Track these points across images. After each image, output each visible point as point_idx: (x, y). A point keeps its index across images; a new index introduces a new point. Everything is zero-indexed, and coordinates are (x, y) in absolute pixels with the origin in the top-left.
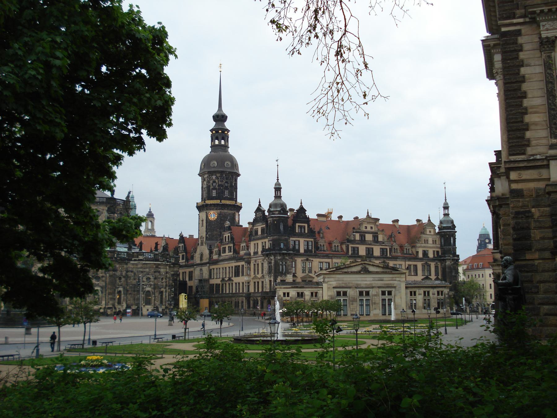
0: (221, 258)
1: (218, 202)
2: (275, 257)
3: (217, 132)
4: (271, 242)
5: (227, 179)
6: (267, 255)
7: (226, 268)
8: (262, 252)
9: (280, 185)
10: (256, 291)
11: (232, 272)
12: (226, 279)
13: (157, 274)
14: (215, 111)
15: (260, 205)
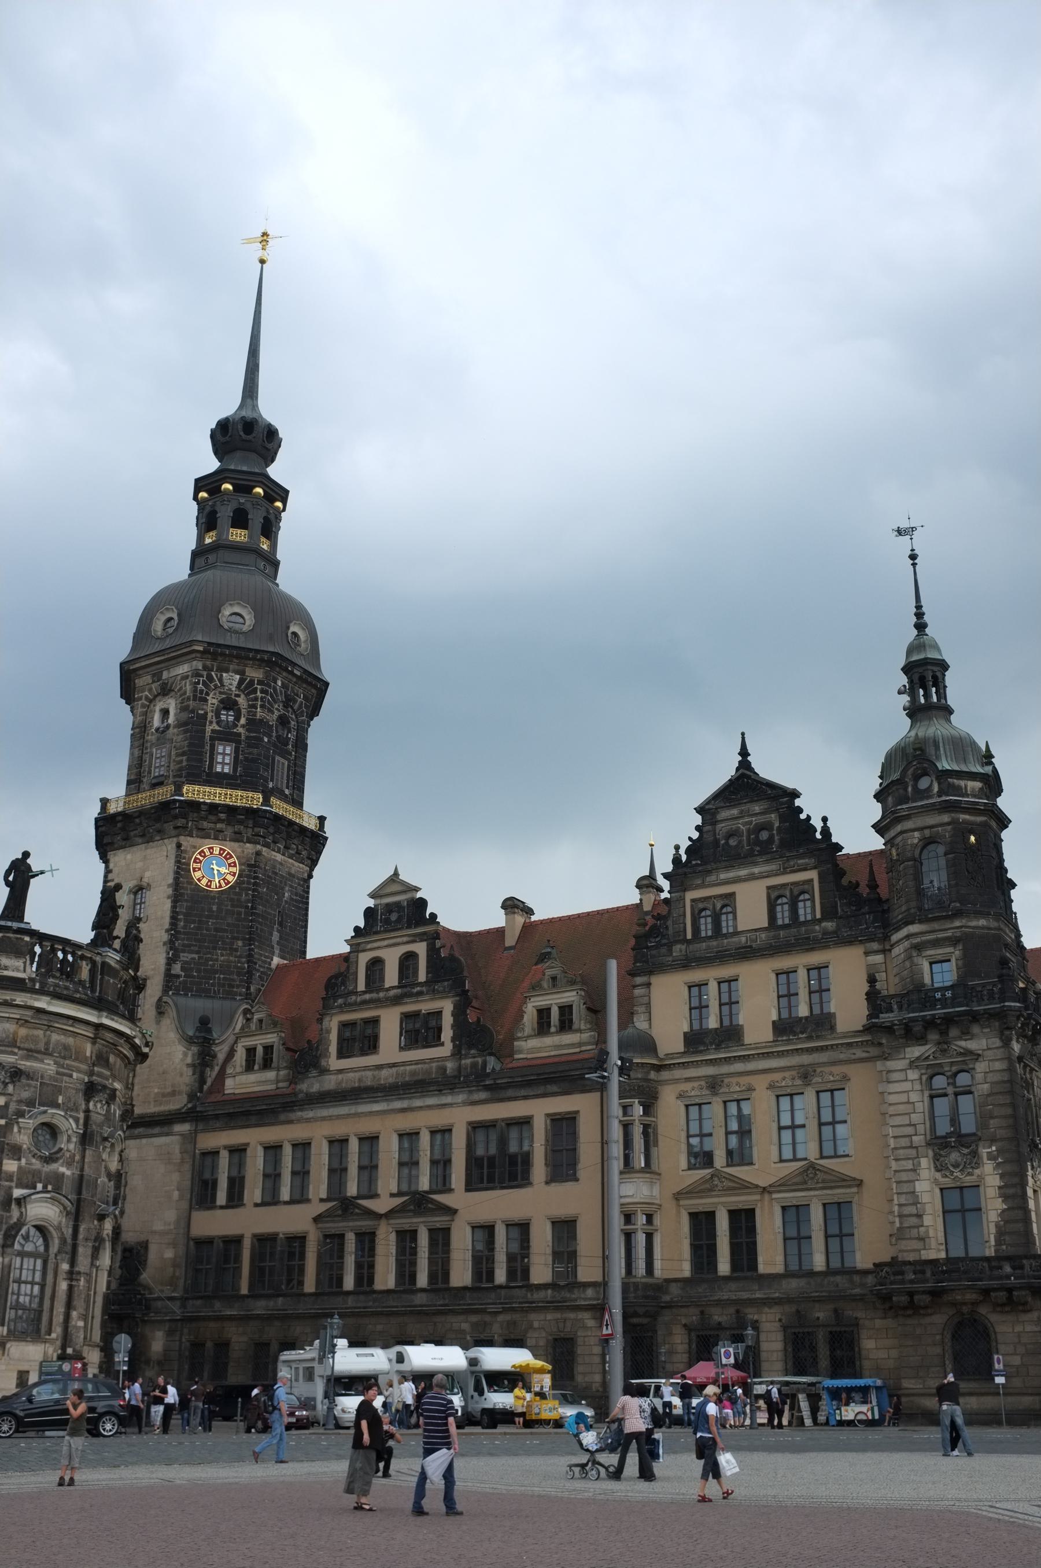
0: (313, 1085)
1: (254, 800)
2: (1006, 1043)
3: (243, 488)
4: (957, 953)
5: (288, 702)
6: (911, 1034)
7: (370, 1141)
8: (783, 1028)
9: (936, 647)
10: (724, 1267)
11: (442, 1164)
12: (382, 1205)
13: (97, 1107)
14: (228, 404)
15: (745, 764)
